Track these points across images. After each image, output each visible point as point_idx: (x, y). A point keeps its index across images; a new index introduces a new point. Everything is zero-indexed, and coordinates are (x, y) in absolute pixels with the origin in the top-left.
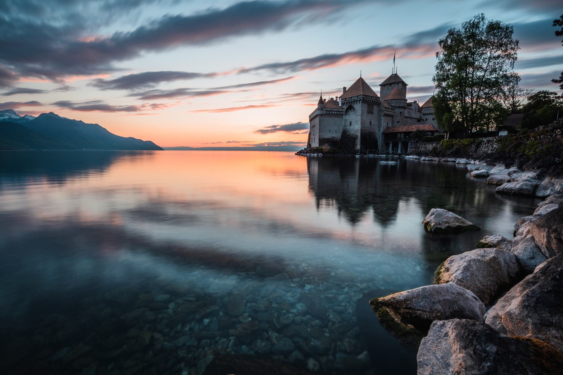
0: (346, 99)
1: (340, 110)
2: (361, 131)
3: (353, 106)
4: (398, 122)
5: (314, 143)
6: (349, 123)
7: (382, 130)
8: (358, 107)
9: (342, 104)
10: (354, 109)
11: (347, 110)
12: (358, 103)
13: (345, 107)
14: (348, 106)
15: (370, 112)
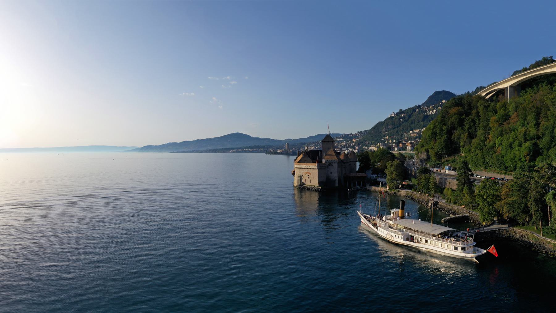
0: (328, 160)
1: (325, 166)
2: (338, 176)
3: (332, 164)
4: (347, 170)
5: (311, 182)
6: (330, 173)
7: (343, 175)
8: (335, 165)
9: (325, 162)
10: (332, 165)
11: (328, 166)
12: (335, 163)
13: (327, 164)
14: (329, 164)
15: (339, 167)
